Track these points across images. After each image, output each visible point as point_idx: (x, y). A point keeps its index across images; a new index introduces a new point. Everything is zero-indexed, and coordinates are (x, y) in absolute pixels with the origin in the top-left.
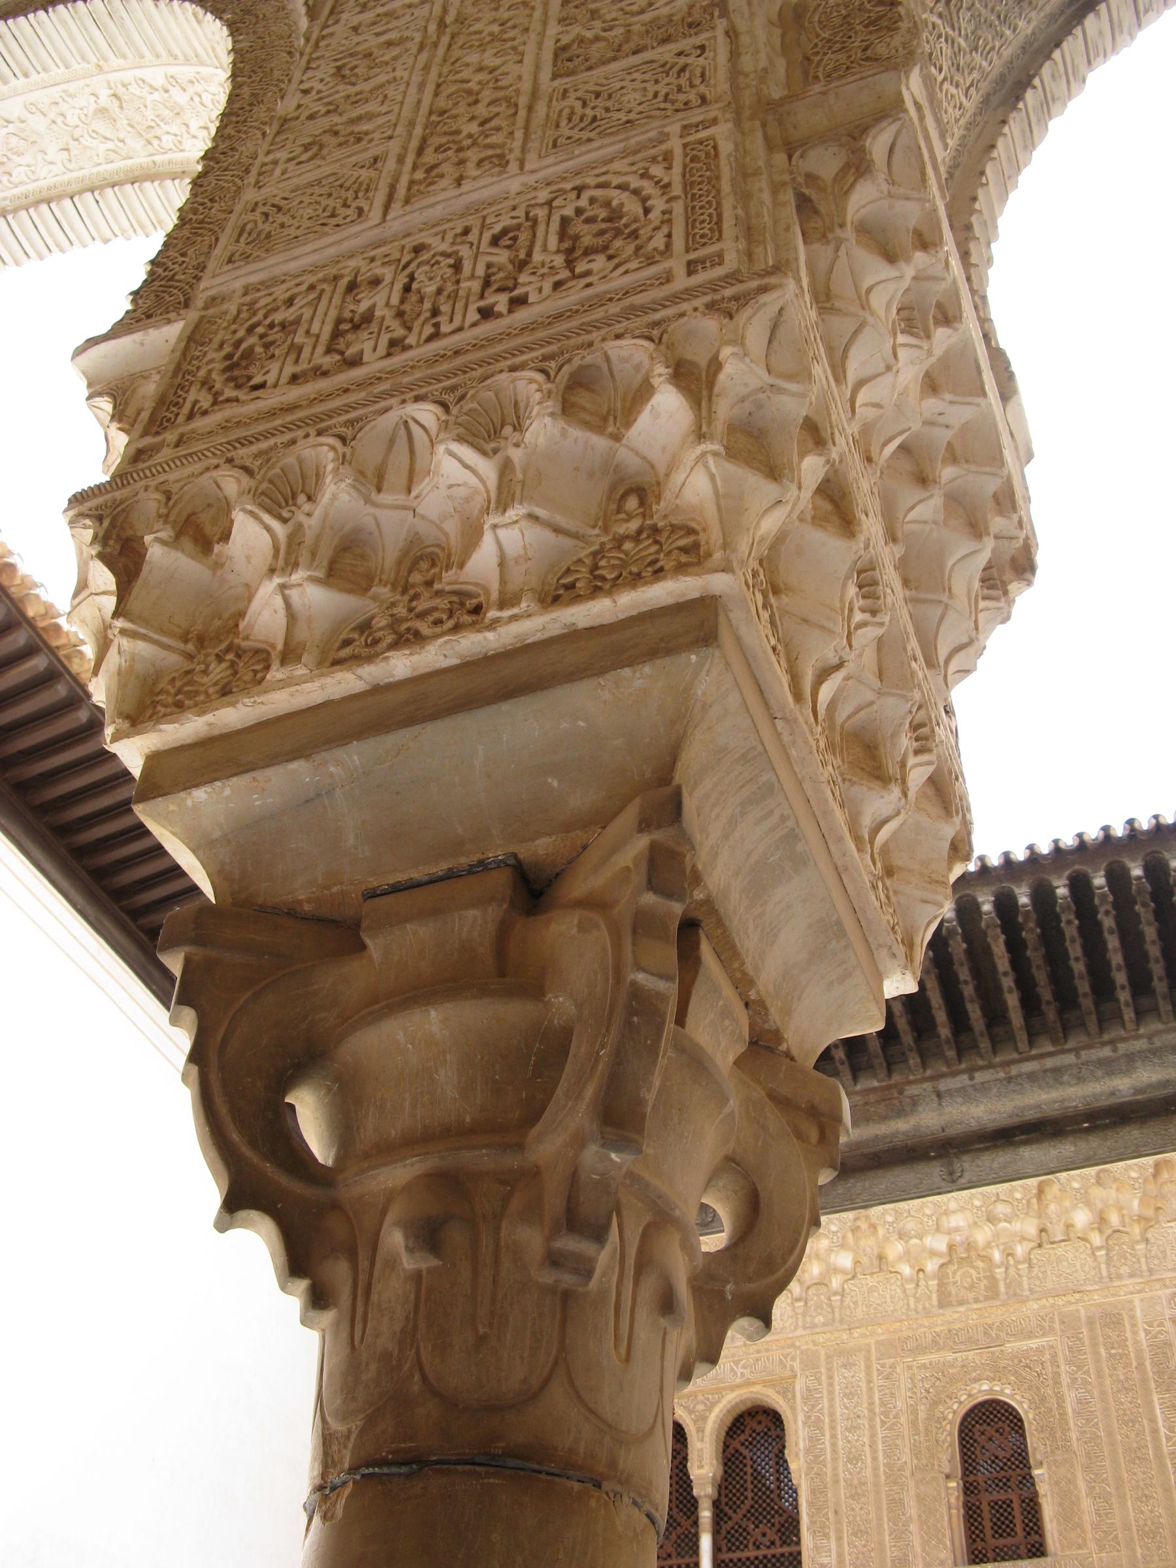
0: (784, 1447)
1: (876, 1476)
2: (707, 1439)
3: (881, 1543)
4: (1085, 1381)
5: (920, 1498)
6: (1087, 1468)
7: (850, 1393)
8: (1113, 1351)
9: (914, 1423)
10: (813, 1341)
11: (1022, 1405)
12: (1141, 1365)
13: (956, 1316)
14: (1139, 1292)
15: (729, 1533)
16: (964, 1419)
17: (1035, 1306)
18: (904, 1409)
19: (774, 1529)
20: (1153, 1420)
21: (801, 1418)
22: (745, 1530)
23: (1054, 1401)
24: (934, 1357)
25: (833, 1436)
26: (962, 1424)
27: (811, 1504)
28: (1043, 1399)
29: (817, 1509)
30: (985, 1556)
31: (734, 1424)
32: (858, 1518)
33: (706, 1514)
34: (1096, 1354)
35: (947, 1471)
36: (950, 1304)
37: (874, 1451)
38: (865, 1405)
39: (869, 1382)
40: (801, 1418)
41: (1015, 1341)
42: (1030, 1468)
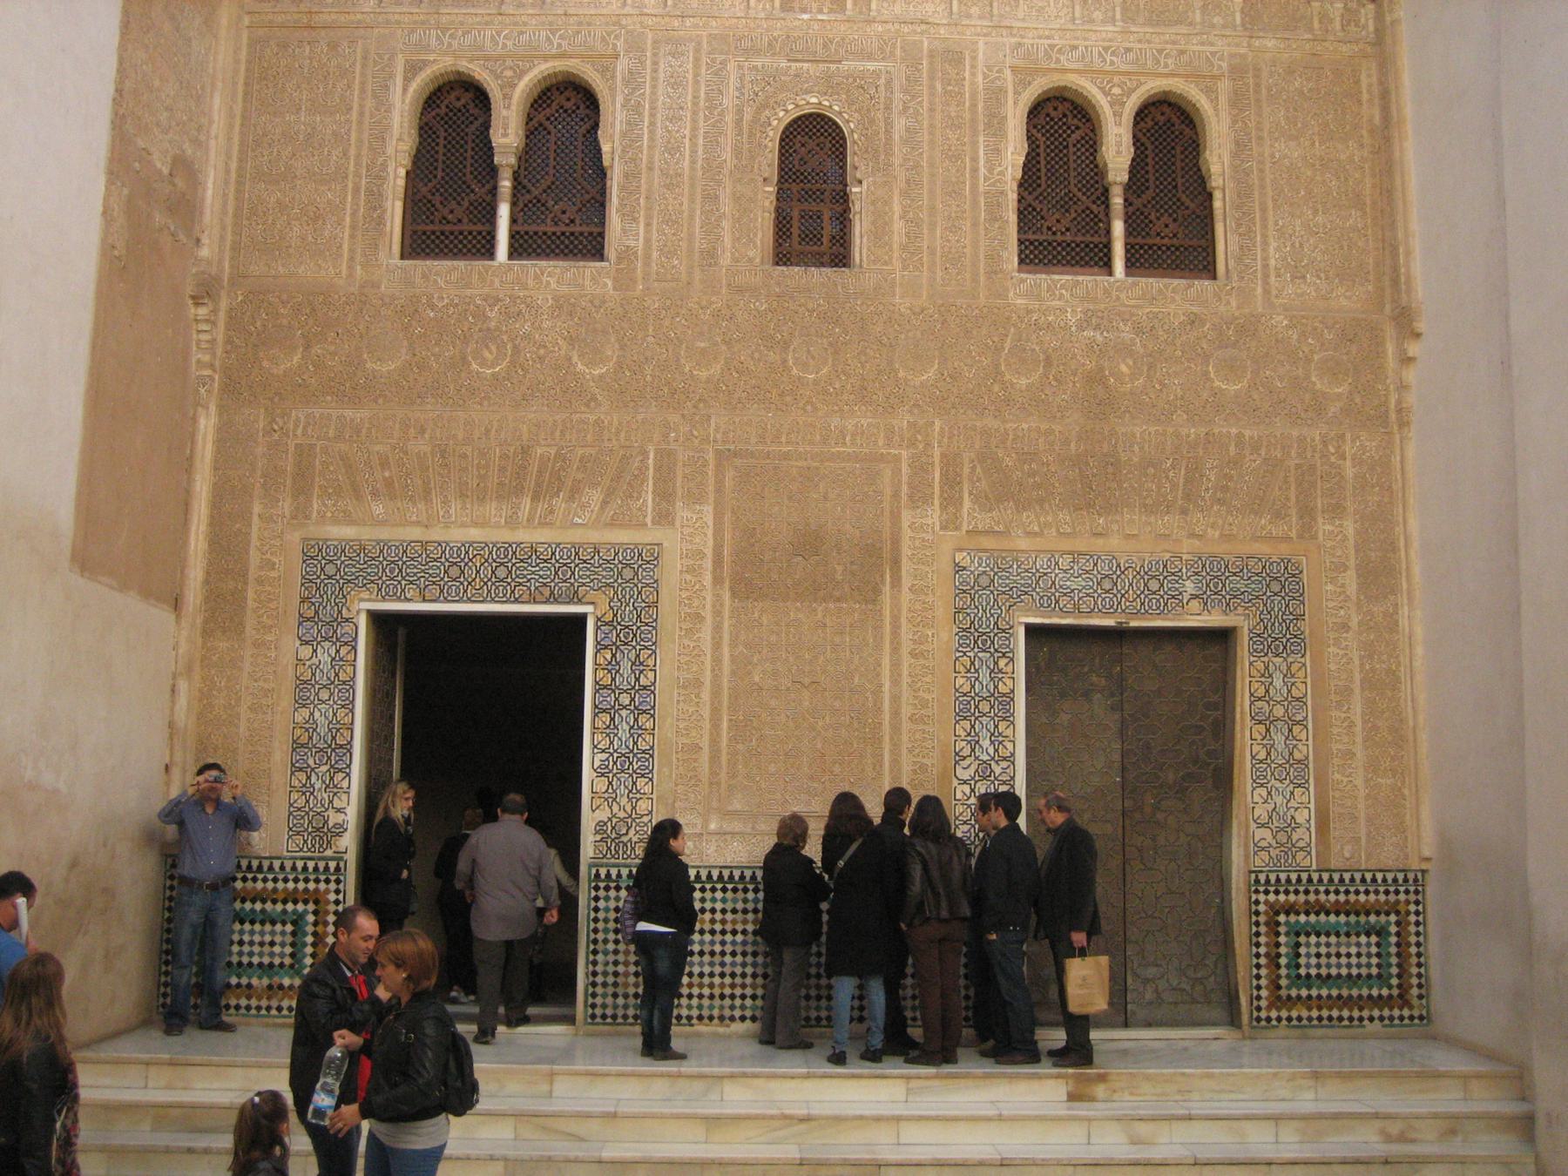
0: (596, 126)
1: (693, 169)
2: (514, 108)
3: (691, 236)
4: (917, 113)
5: (737, 198)
6: (905, 194)
7: (676, 83)
8: (950, 88)
9: (739, 123)
10: (641, 23)
11: (850, 126)
12: (974, 105)
13: (797, 23)
14: (985, 35)
15: (526, 205)
16: (786, 128)
17: (880, 29)
18: (730, 108)
19: (576, 208)
20: (975, 159)
21: (620, 99)
22: (543, 205)
23: (882, 124)
24: (767, 61)
25: (652, 124)
26: (783, 132)
27: (622, 188)
28: (872, 122)
29: (628, 190)
30: (789, 260)
31: (540, 98)
32: (670, 208)
33: (506, 184)
34: (932, 87)
35: (766, 175)
36: (791, 9)
37: (694, 145)
38: (690, 97)
39: (696, 75)
40: (620, 99)
41: (853, 60)
42: (846, 185)
